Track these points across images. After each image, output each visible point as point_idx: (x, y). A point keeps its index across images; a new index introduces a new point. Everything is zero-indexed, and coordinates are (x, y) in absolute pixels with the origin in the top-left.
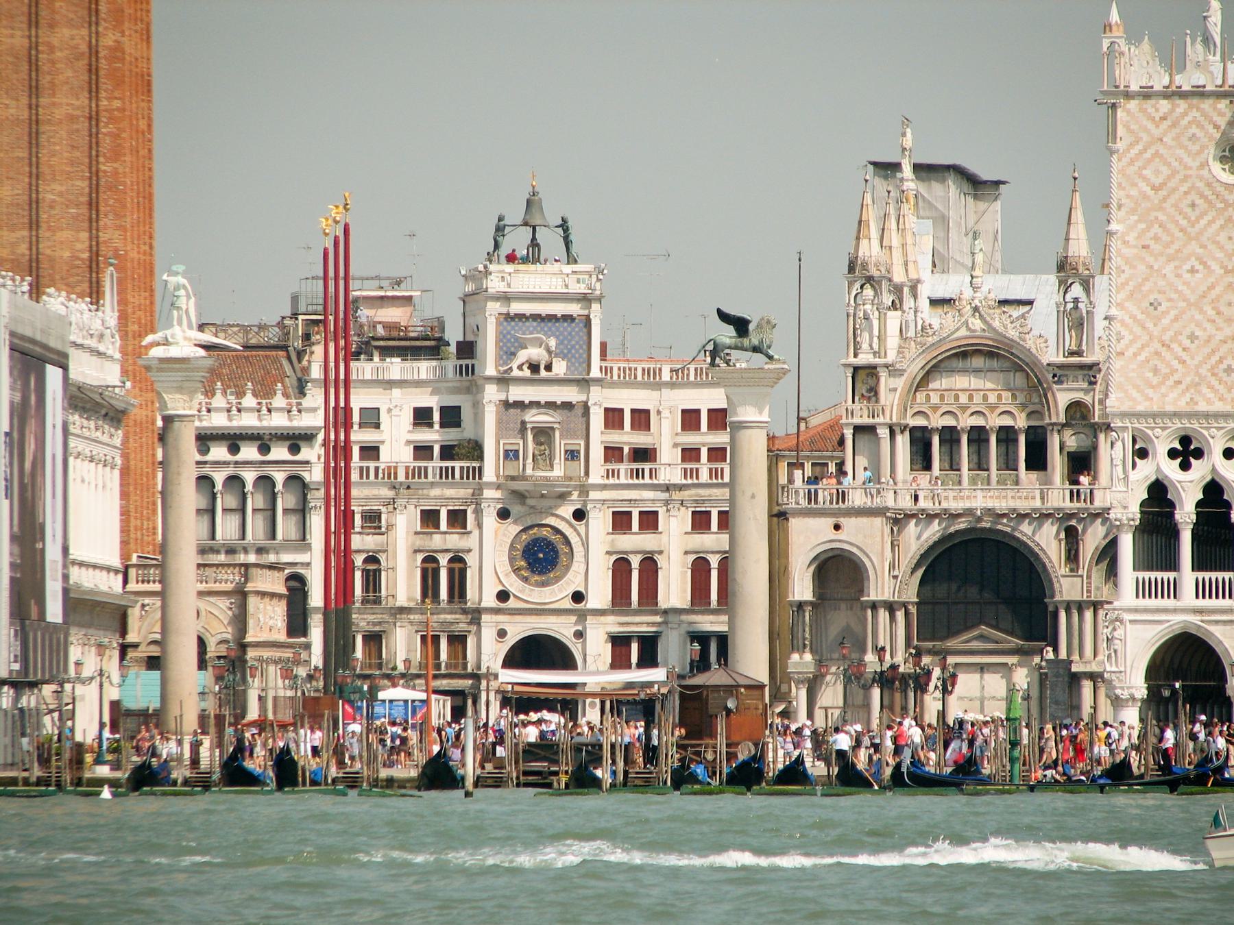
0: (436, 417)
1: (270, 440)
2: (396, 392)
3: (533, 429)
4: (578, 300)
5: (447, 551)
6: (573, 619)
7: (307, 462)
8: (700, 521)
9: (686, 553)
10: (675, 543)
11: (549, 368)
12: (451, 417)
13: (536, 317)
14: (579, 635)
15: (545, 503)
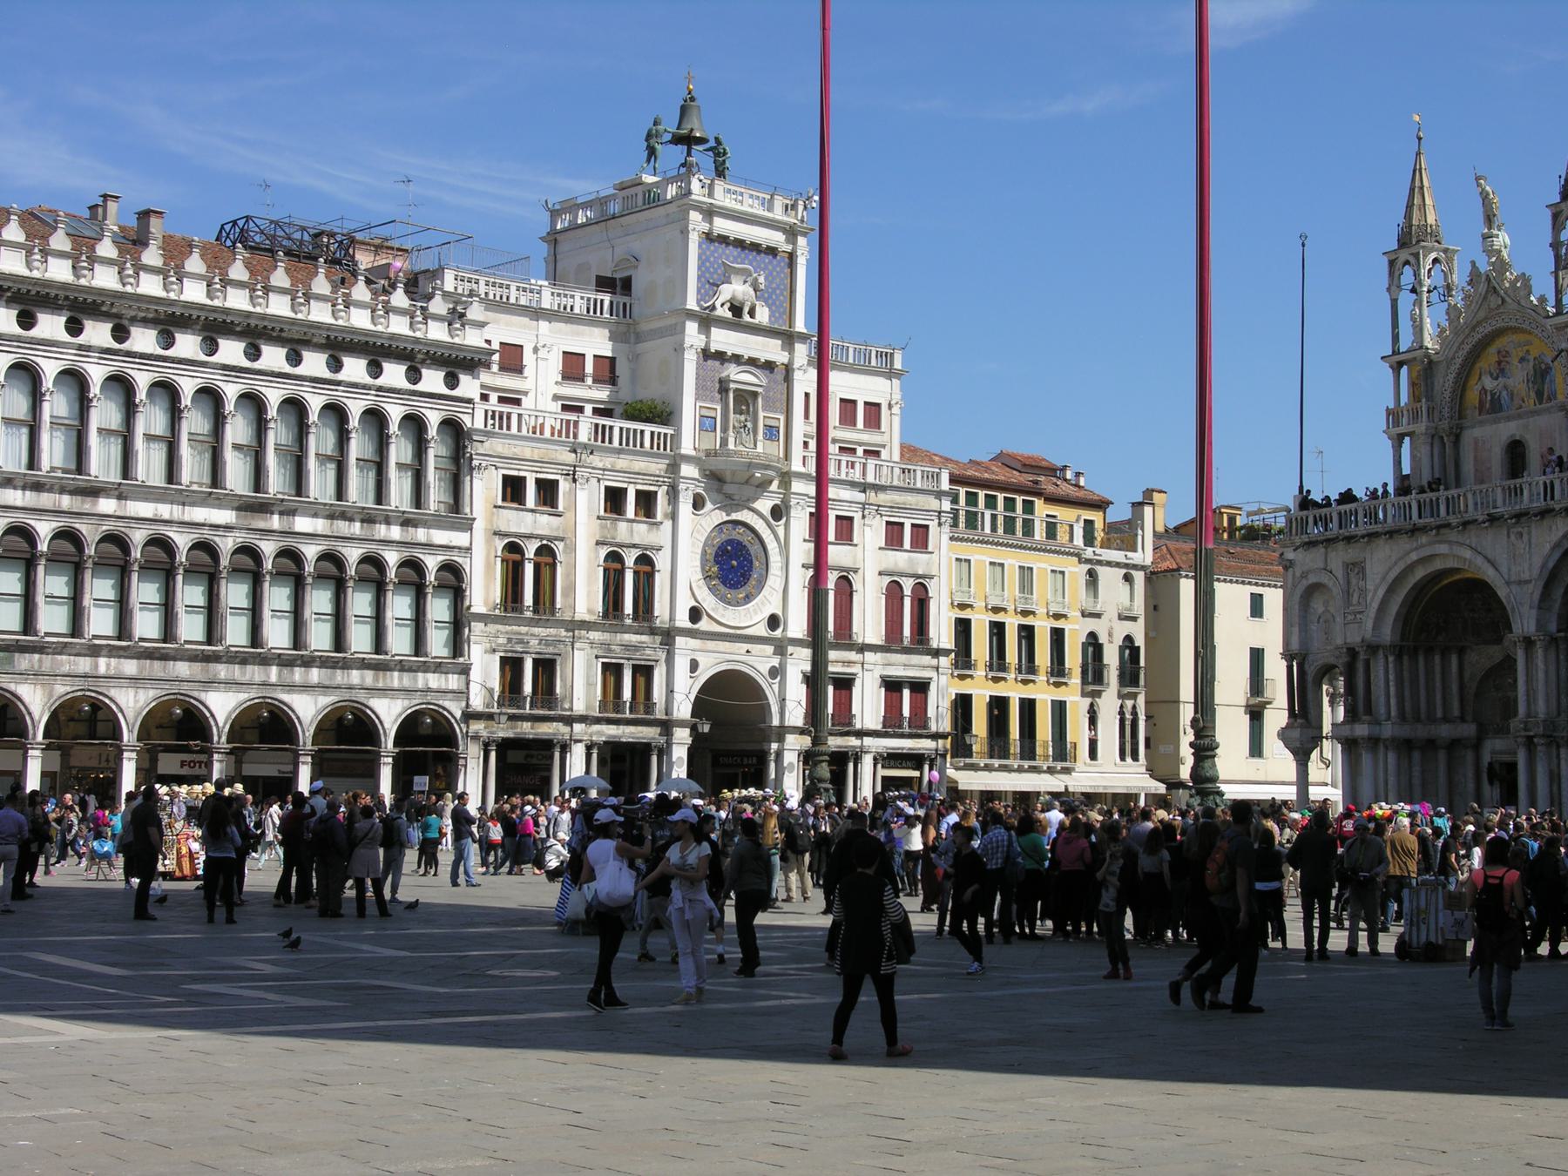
0: (589, 368)
1: (423, 362)
2: (543, 325)
3: (736, 390)
4: (784, 231)
5: (634, 546)
6: (770, 649)
7: (470, 401)
8: (894, 535)
9: (880, 574)
10: (867, 558)
11: (752, 313)
12: (608, 371)
13: (740, 244)
14: (774, 672)
15: (748, 491)
